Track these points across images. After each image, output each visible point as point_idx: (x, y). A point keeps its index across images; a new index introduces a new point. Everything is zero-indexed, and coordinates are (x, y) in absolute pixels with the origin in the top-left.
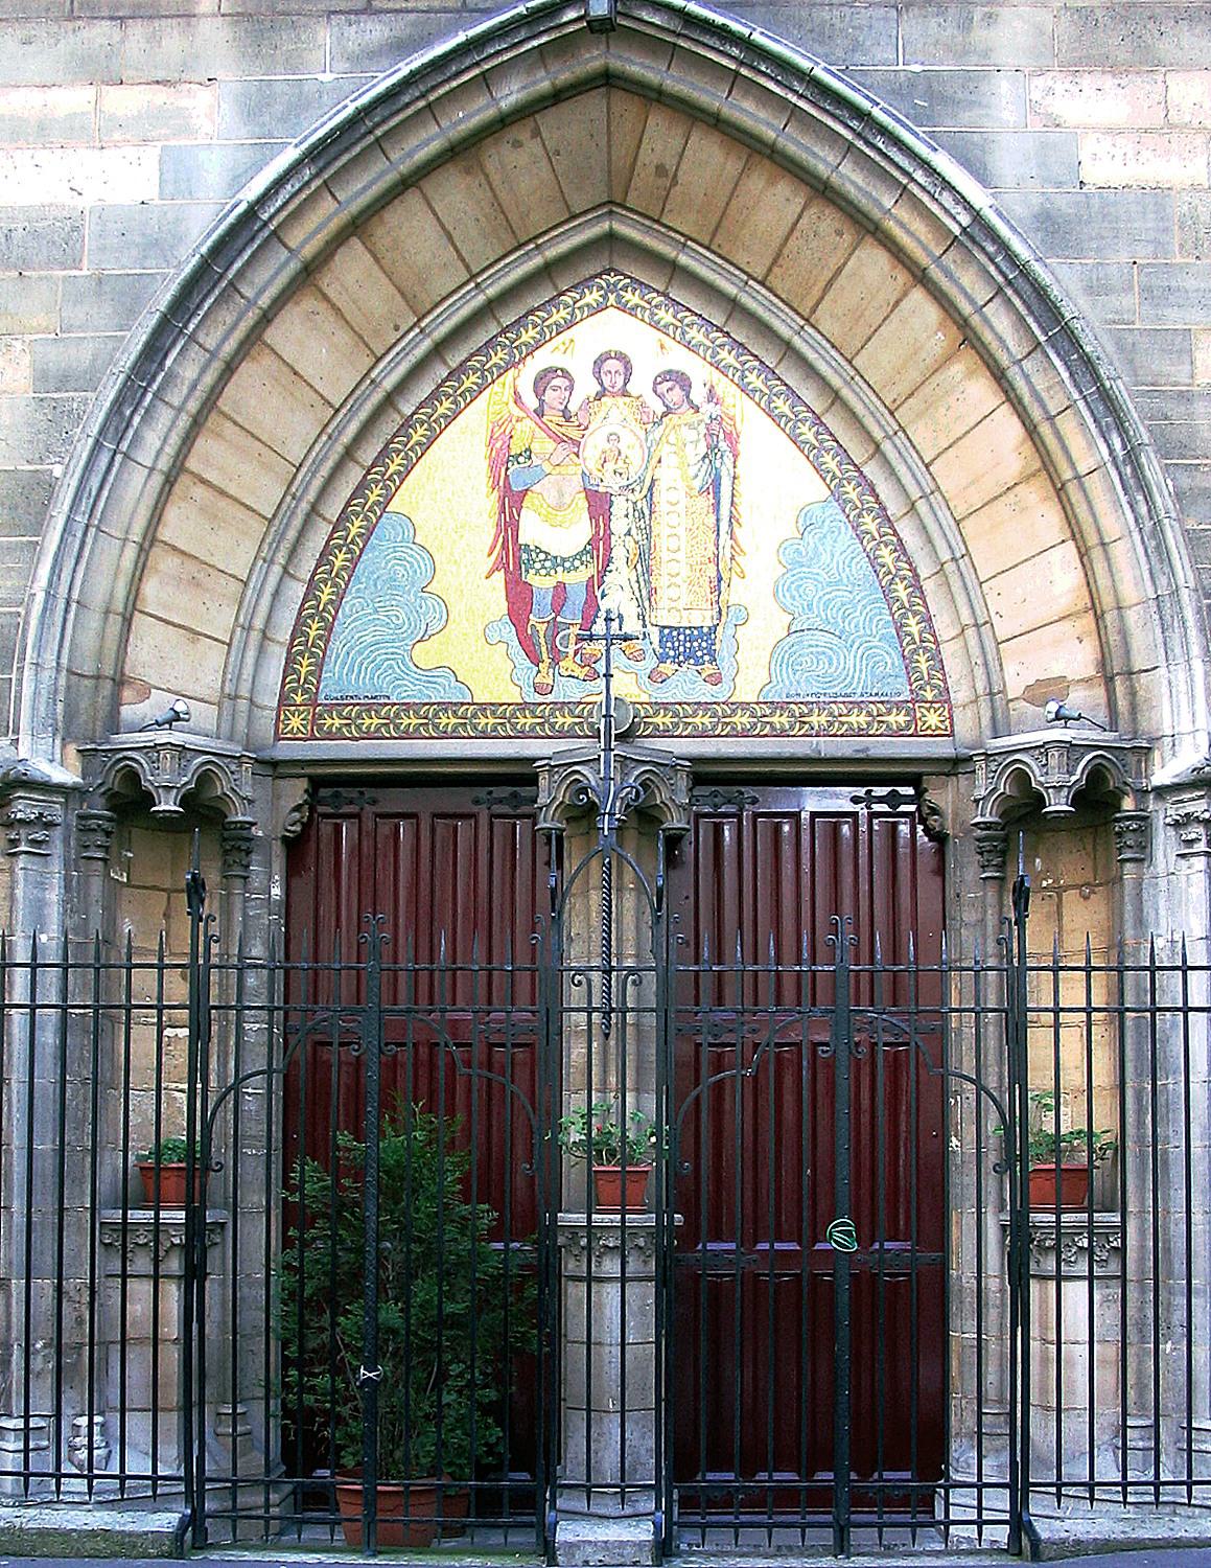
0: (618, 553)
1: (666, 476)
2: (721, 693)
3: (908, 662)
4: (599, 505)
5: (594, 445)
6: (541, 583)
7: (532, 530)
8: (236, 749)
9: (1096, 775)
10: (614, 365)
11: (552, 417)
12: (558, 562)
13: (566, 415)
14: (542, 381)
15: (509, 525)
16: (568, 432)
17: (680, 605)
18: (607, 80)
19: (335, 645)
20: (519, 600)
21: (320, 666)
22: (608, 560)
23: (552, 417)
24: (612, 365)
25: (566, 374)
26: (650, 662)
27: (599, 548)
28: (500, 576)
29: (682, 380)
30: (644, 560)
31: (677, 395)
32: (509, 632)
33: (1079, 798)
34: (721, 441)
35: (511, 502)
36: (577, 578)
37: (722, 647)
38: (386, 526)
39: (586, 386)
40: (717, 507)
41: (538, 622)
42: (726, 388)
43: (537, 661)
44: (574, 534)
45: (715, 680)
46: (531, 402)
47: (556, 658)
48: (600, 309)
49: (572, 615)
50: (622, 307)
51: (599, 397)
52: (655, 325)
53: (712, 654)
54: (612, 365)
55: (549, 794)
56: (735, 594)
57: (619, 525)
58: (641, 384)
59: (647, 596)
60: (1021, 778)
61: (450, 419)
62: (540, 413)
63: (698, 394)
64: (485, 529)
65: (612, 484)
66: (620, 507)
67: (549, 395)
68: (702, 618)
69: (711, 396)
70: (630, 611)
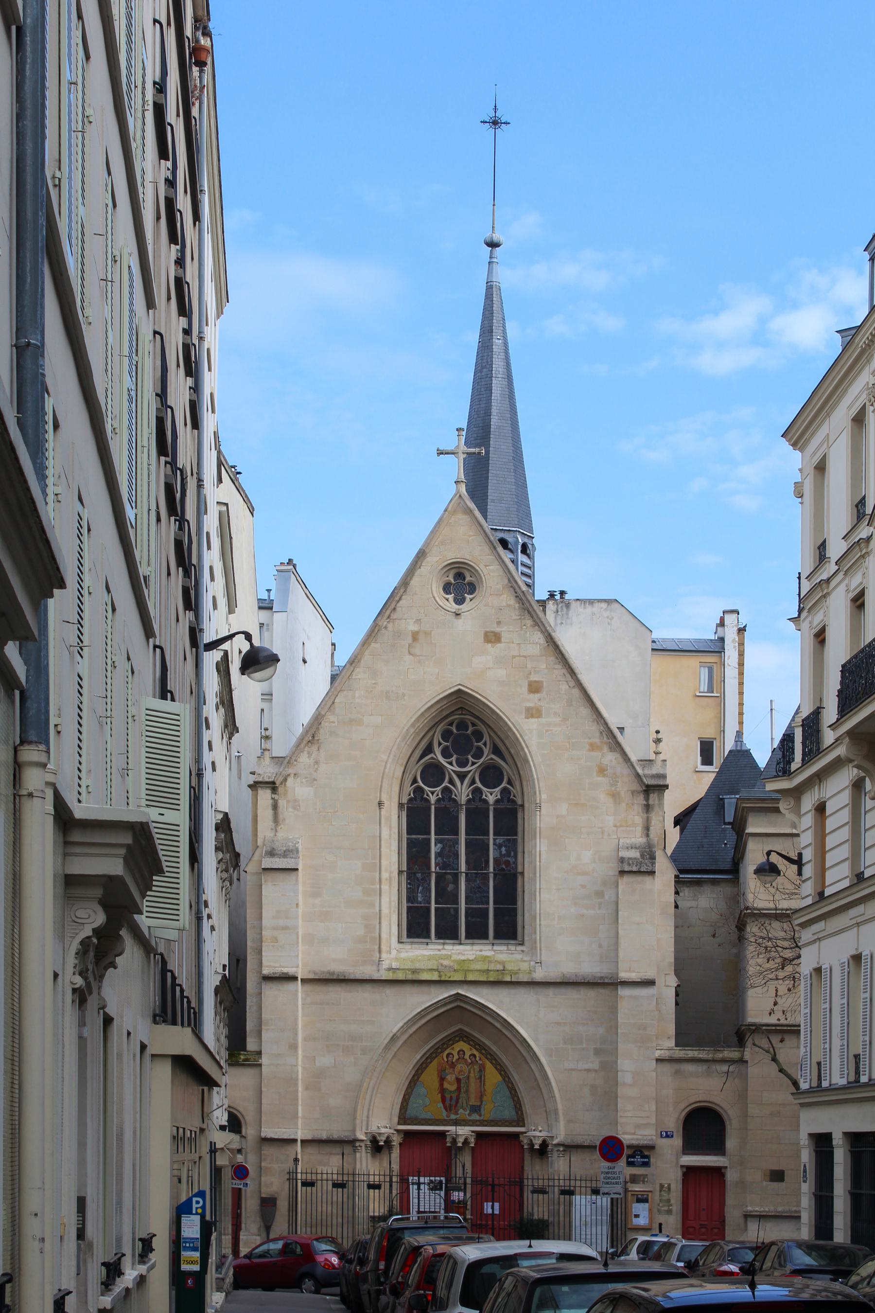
0: (462, 1090)
1: (472, 1075)
2: (482, 1118)
3: (517, 1113)
4: (458, 1080)
5: (458, 1067)
6: (447, 1096)
7: (446, 1085)
8: (392, 1131)
9: (544, 1141)
10: (461, 1052)
11: (450, 1063)
12: (451, 1092)
13: (453, 1063)
14: (448, 1056)
15: (441, 1085)
16: (453, 1065)
17: (473, 1102)
18: (458, 1007)
19: (409, 1107)
20: (443, 1100)
21: (406, 1111)
22: (460, 1091)
23: (450, 1063)
24: (461, 1052)
25: (452, 1054)
26: (468, 1112)
27: (459, 1089)
28: (440, 1095)
29: (474, 1056)
30: (467, 1091)
31: (473, 1059)
32: (441, 1105)
33: (541, 1145)
34: (482, 1068)
35: (442, 1079)
36: (454, 1096)
37: (482, 1110)
38: (418, 1083)
39: (456, 1057)
40: (481, 1082)
41: (448, 1102)
42: (483, 1058)
43: (446, 1110)
44: (453, 1088)
45: (480, 1115)
46: (445, 1059)
47: (450, 1110)
48: (458, 1041)
49: (453, 1103)
50: (463, 1041)
51: (459, 1058)
52: (469, 1044)
53: (480, 1110)
54: (461, 1052)
55: (449, 1139)
56: (485, 1098)
57: (462, 1085)
58: (467, 1057)
59: (468, 1099)
60: (531, 1140)
61: (430, 1063)
62: (447, 1062)
63: (478, 1059)
64: (436, 1085)
65: (461, 1077)
66: (463, 1081)
67: (449, 1059)
68: (479, 1104)
69: (480, 1059)
70: (465, 1102)
